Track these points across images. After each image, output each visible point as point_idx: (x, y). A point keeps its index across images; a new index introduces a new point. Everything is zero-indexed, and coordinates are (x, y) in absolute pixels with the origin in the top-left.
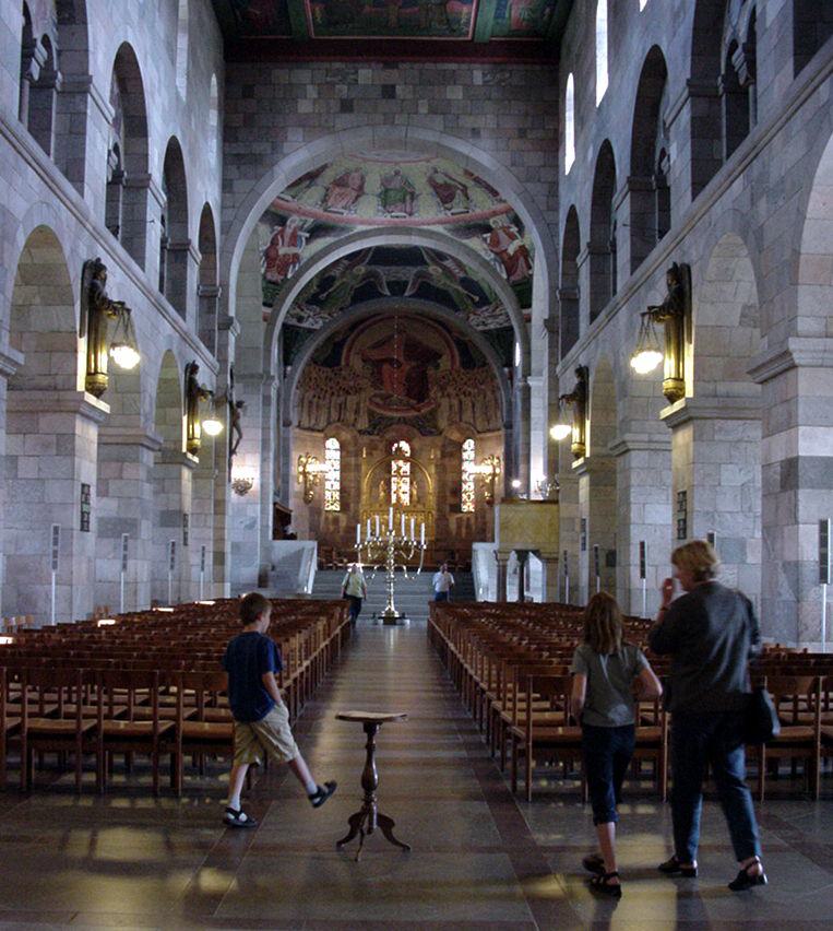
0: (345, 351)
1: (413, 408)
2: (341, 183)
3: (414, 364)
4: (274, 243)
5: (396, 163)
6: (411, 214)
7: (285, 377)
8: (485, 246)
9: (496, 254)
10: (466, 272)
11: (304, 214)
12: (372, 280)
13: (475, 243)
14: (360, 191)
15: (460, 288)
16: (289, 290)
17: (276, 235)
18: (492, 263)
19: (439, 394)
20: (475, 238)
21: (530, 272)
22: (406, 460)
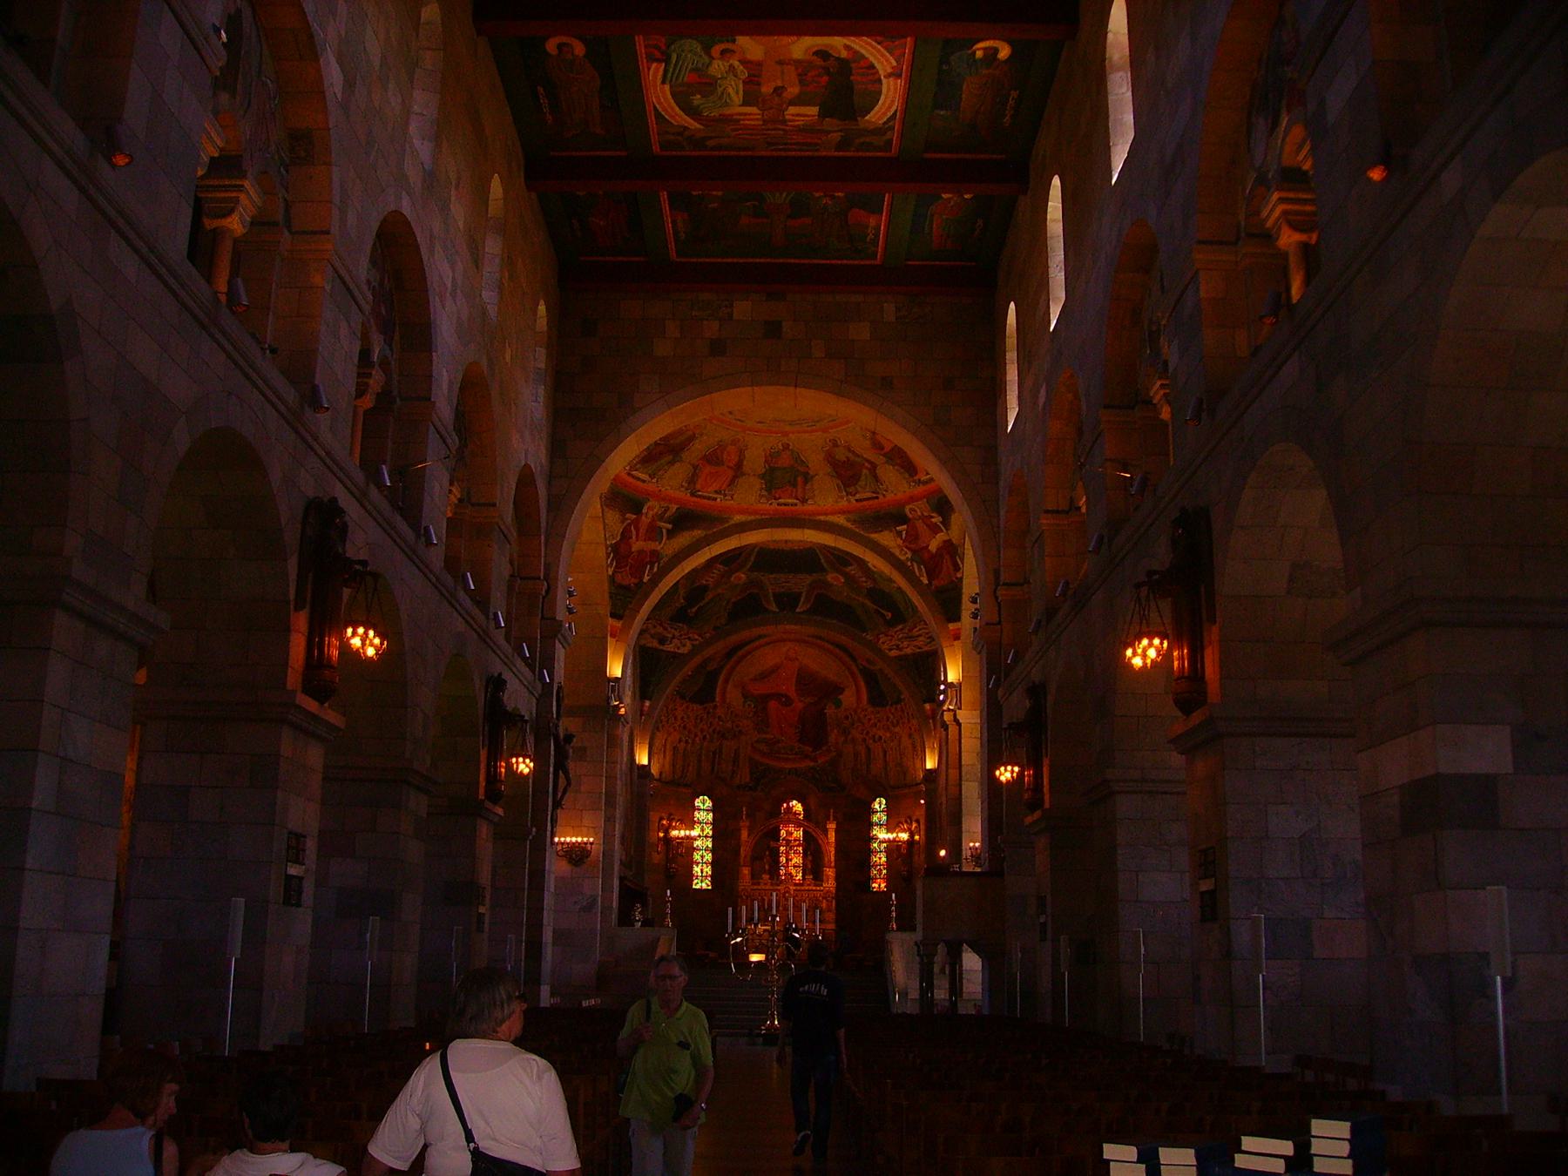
2: (713, 458)
4: (625, 535)
5: (786, 434)
6: (804, 501)
7: (641, 715)
8: (900, 541)
9: (914, 552)
10: (874, 580)
11: (664, 499)
12: (756, 591)
13: (886, 539)
14: (738, 469)
15: (868, 603)
16: (646, 597)
17: (629, 525)
18: (909, 564)
20: (886, 533)
21: (959, 575)
22: (798, 825)
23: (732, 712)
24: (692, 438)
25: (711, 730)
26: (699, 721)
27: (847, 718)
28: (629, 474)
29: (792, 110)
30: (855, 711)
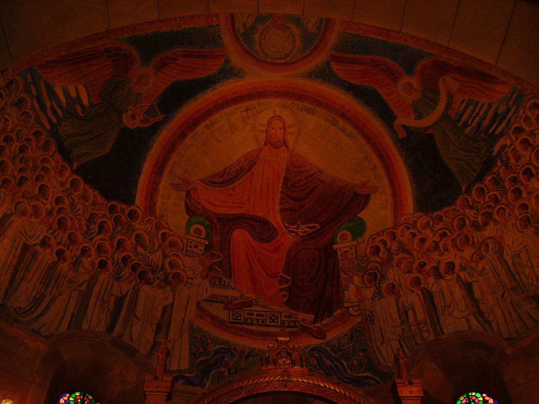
0: (147, 168)
1: (305, 330)
3: (304, 229)
19: (369, 292)
23: (164, 234)
25: (119, 256)
26: (95, 228)
27: (376, 250)
30: (393, 237)
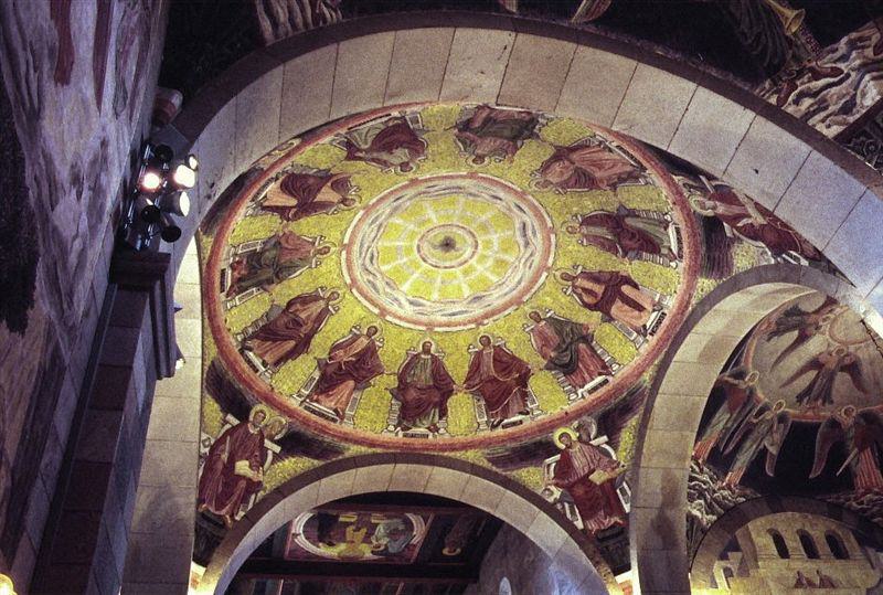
2: (584, 180)
5: (472, 176)
24: (588, 221)
28: (681, 257)
29: (353, 520)
